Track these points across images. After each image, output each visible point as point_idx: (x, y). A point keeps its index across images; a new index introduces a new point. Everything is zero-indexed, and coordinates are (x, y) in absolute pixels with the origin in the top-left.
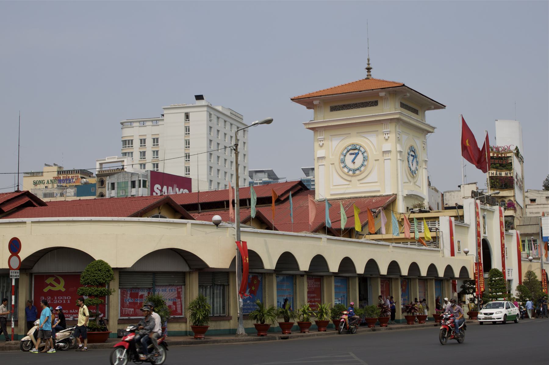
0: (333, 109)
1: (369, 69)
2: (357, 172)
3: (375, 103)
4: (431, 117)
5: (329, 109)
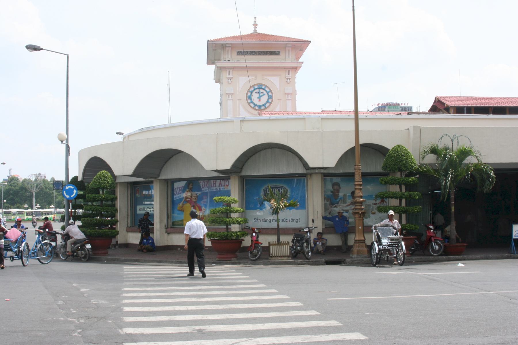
0: (240, 53)
1: (255, 25)
2: (263, 108)
5: (236, 53)
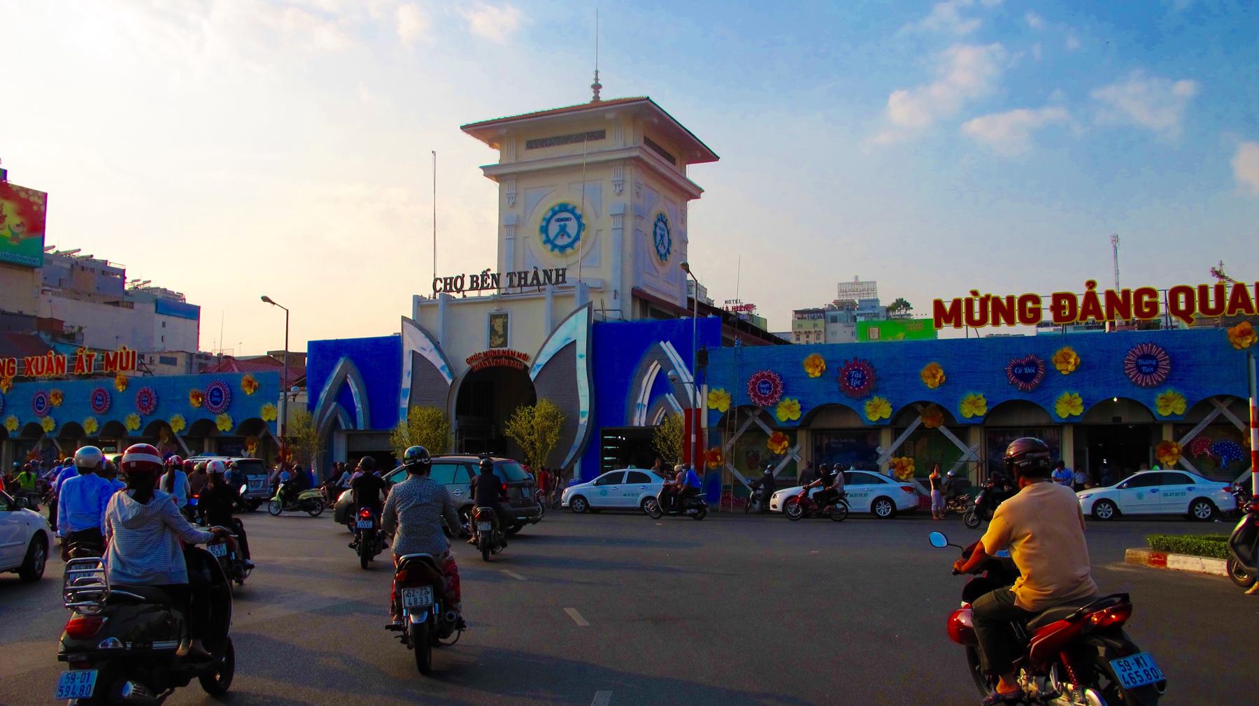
0: (531, 145)
1: (597, 87)
2: (569, 250)
3: (600, 135)
4: (695, 172)
5: (523, 146)
